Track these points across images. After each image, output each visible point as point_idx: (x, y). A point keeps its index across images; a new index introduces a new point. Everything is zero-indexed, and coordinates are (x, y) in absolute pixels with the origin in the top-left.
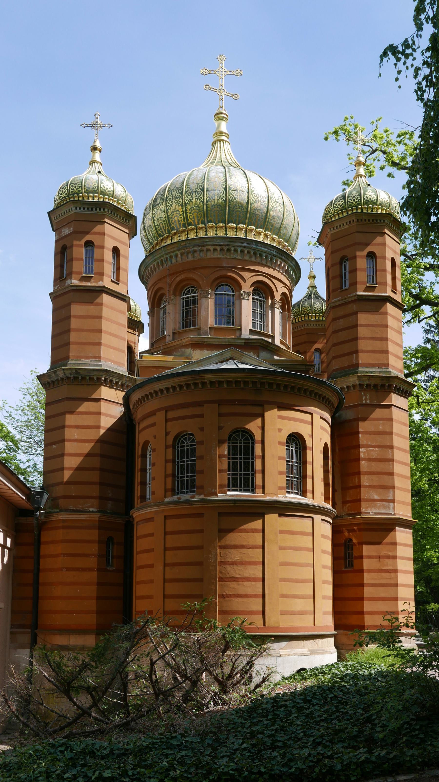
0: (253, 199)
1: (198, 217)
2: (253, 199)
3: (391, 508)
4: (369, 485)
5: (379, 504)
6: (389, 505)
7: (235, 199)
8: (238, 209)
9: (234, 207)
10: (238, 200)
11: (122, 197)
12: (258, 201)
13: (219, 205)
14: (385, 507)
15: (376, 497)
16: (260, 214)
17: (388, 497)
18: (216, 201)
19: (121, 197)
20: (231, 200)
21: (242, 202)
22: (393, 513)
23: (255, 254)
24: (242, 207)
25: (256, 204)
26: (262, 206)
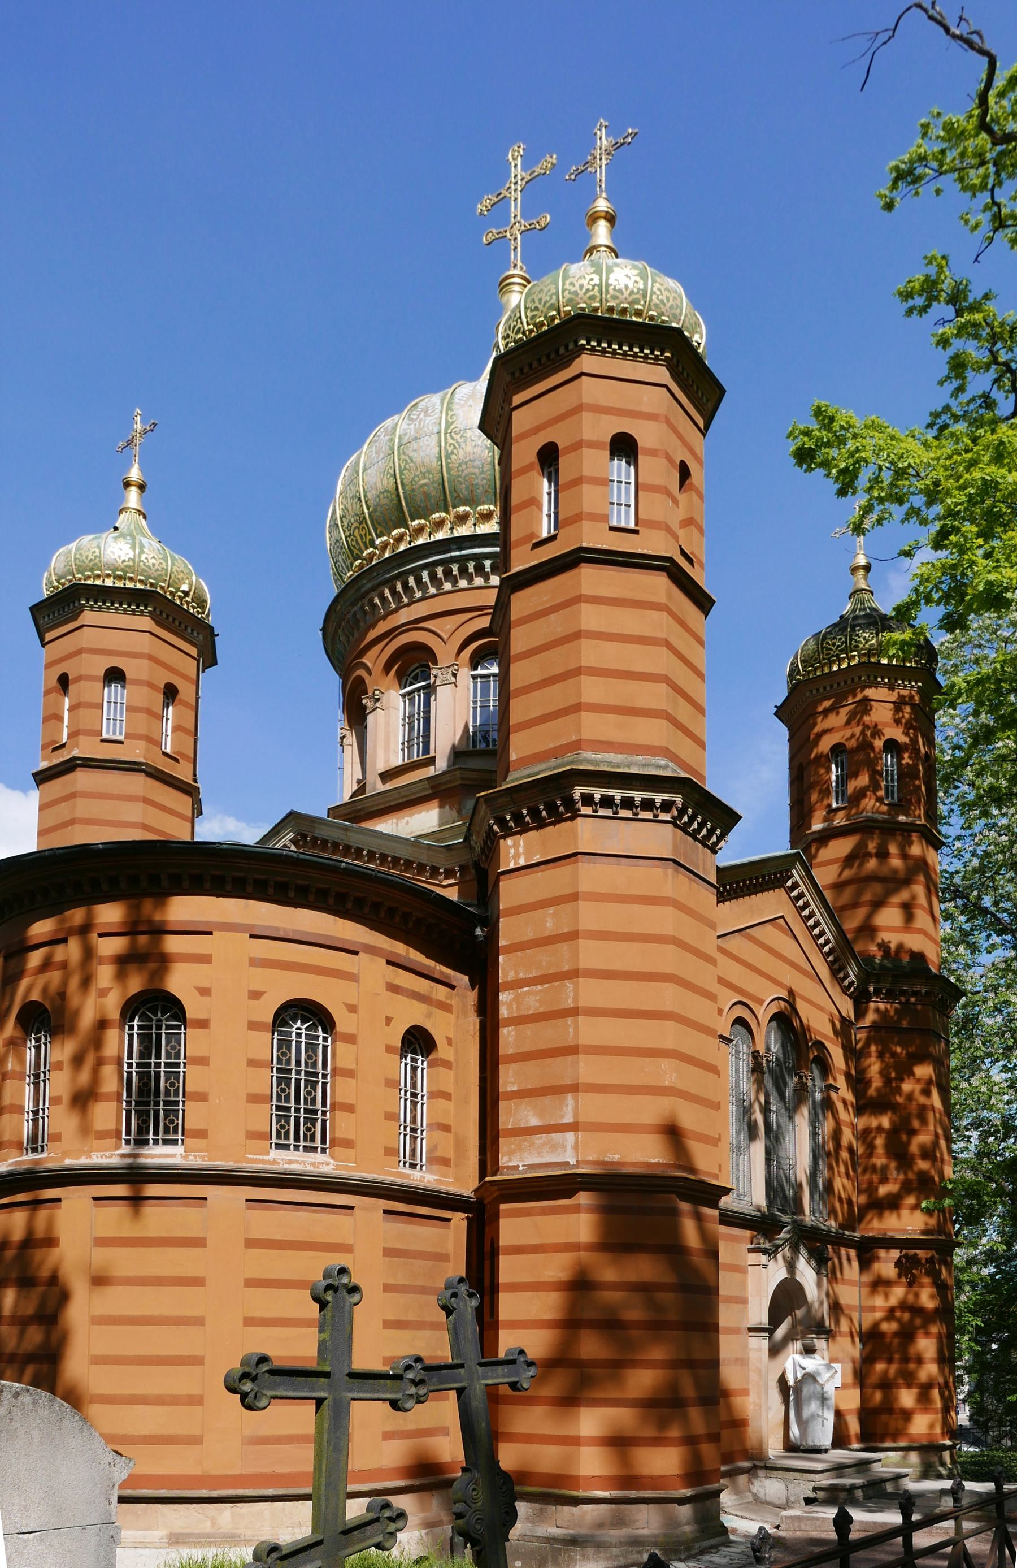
0: (450, 441)
1: (361, 536)
2: (450, 441)
3: (569, 1149)
4: (518, 1091)
5: (539, 1139)
6: (565, 1140)
7: (412, 460)
8: (422, 482)
9: (413, 479)
10: (419, 460)
11: (124, 561)
12: (465, 441)
13: (386, 491)
14: (554, 1147)
15: (534, 1122)
16: (477, 470)
17: (562, 1117)
18: (379, 485)
19: (120, 562)
20: (405, 468)
21: (427, 461)
22: (573, 1162)
23: (463, 571)
24: (429, 472)
25: (461, 451)
26: (476, 450)
